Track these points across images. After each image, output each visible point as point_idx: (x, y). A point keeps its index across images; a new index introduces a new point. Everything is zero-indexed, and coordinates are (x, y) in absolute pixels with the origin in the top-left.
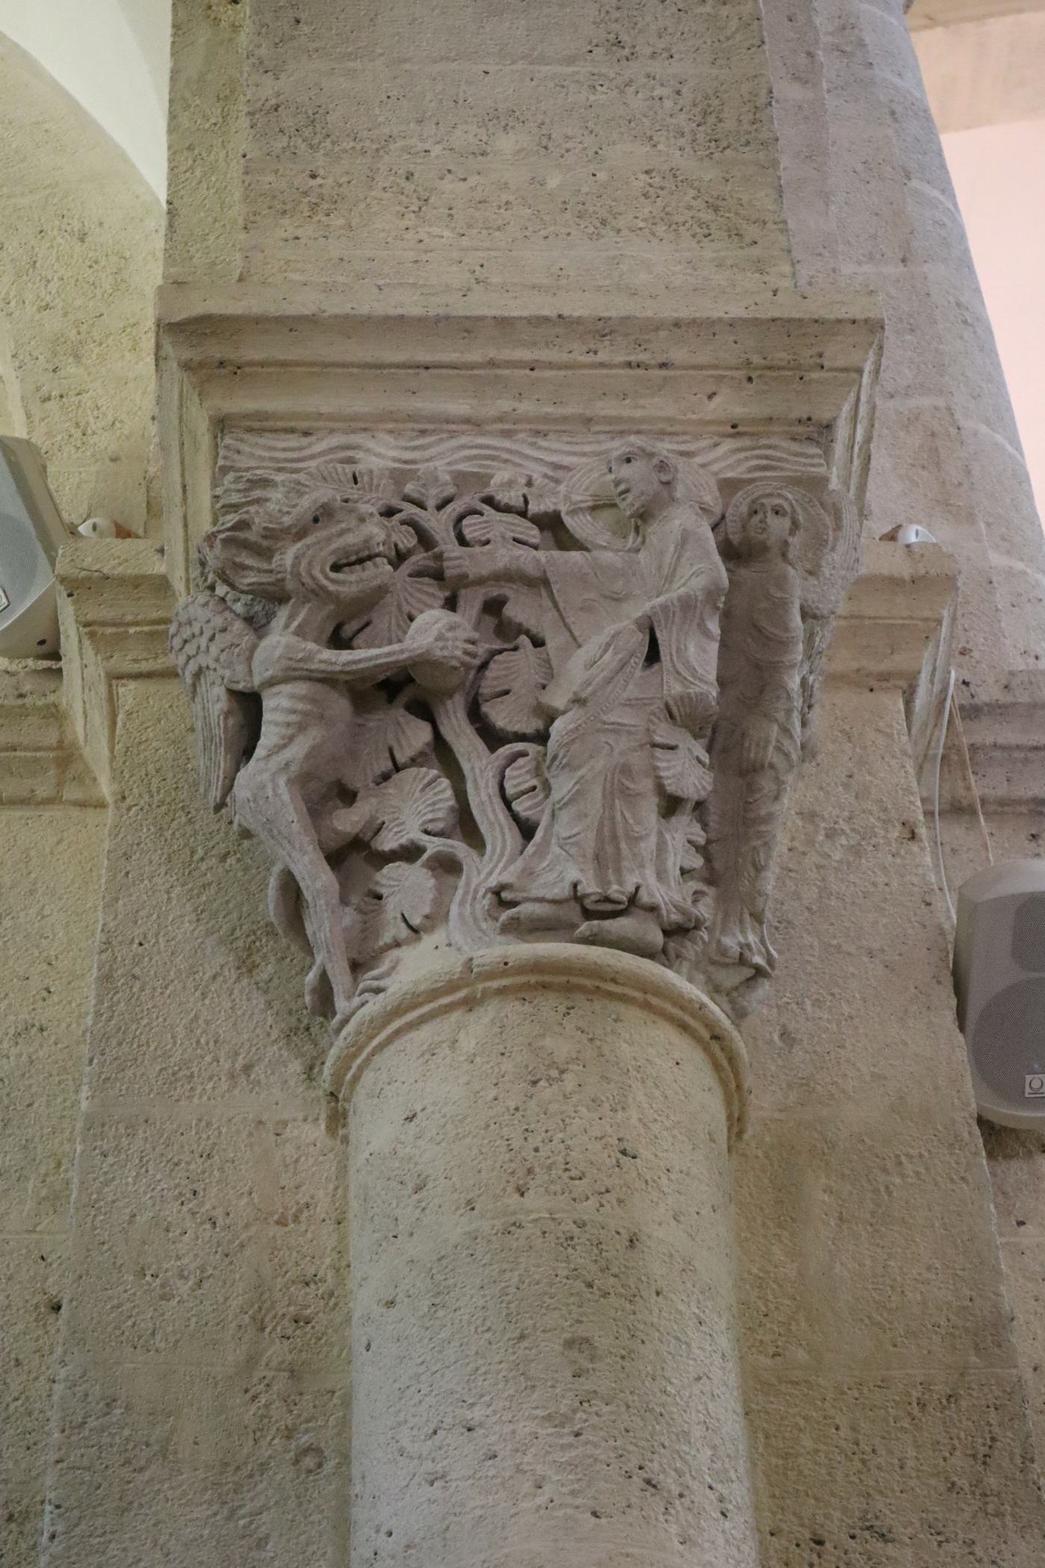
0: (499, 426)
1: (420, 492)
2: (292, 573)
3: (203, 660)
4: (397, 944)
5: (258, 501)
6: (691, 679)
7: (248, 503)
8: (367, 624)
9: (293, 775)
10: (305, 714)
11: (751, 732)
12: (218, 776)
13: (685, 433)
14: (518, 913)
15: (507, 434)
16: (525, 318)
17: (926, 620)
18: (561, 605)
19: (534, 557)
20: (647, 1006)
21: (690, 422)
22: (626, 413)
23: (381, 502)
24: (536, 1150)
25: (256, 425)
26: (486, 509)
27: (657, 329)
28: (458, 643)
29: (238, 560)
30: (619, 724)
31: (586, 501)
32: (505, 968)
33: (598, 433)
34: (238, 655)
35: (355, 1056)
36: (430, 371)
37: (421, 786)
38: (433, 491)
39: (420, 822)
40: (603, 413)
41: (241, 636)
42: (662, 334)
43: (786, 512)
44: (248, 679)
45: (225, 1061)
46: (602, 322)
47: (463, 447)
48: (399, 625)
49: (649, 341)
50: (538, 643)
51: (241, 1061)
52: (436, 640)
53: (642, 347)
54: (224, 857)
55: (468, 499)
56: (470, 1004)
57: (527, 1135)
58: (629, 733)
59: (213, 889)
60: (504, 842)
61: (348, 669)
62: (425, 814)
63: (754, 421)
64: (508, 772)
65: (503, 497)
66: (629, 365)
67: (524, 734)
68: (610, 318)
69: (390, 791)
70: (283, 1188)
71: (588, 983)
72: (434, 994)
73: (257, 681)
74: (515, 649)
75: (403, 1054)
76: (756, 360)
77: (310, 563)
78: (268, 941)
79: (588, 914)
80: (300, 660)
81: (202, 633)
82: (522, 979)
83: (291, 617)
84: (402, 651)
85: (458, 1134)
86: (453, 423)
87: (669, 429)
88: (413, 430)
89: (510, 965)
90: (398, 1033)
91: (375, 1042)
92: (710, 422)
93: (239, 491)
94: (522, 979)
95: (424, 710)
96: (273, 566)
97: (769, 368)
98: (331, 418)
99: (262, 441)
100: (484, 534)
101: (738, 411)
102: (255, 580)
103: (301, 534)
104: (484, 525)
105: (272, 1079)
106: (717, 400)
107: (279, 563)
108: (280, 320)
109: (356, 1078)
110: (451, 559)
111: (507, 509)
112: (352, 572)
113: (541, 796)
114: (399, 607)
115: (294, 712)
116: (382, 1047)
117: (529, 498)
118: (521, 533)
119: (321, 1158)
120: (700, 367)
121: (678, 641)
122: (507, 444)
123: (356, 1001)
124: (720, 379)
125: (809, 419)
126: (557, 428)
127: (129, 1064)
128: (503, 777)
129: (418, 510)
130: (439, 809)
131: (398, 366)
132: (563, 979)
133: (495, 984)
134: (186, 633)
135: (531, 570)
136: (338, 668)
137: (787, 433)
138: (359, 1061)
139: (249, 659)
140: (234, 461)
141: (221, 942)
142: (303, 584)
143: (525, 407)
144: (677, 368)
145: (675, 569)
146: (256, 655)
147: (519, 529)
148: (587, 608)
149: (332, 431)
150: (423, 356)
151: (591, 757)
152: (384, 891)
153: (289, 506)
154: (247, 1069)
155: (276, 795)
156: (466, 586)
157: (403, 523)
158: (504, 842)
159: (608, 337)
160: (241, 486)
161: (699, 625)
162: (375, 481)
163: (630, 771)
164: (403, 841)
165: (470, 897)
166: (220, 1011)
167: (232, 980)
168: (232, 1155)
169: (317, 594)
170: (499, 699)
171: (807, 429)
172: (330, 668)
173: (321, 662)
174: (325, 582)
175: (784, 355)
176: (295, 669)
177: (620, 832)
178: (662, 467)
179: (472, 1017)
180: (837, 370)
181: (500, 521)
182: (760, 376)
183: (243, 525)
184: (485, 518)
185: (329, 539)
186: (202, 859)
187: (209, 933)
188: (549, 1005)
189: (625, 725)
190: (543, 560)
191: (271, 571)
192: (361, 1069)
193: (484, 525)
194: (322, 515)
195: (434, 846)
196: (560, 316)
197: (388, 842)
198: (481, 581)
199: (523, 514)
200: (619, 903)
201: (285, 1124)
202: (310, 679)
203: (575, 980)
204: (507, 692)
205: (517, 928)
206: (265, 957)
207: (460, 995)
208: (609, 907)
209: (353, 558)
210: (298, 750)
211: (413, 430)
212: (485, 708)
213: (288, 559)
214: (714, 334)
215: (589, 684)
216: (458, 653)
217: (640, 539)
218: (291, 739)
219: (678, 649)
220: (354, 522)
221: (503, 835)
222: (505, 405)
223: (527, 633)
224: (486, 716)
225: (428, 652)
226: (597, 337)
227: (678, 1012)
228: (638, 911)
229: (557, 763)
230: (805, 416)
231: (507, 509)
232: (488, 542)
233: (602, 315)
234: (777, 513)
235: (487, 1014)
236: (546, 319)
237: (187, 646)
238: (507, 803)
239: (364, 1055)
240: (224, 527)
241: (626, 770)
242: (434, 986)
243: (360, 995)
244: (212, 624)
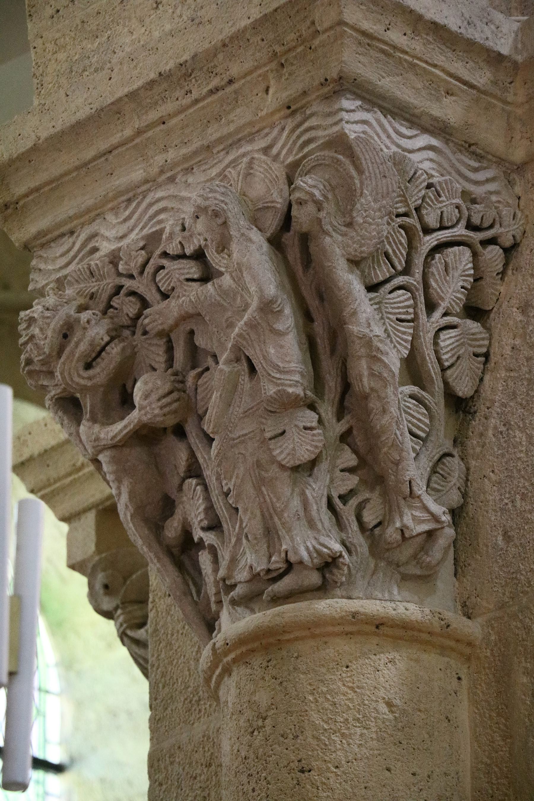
0: (164, 177)
6: (278, 376)
13: (264, 128)
14: (232, 597)
16: (142, 87)
20: (314, 636)
21: (262, 119)
22: (225, 131)
23: (110, 286)
25: (44, 240)
27: (215, 55)
28: (153, 406)
29: (40, 383)
30: (243, 435)
38: (132, 265)
42: (220, 56)
49: (215, 66)
58: (251, 439)
63: (295, 100)
66: (212, 92)
68: (186, 61)
74: (207, 369)
76: (278, 49)
87: (254, 130)
88: (123, 202)
92: (272, 114)
94: (238, 652)
97: (289, 50)
100: (169, 284)
101: (285, 96)
104: (167, 277)
108: (20, 158)
117: (183, 243)
118: (188, 273)
121: (261, 350)
125: (326, 80)
127: (169, 701)
143: (171, 155)
150: (103, 146)
151: (235, 468)
161: (270, 330)
171: (329, 88)
178: (216, 214)
180: (326, 30)
181: (175, 269)
182: (286, 60)
185: (72, 353)
189: (246, 435)
193: (167, 277)
198: (176, 325)
200: (280, 568)
202: (109, 448)
208: (274, 574)
211: (123, 202)
216: (157, 411)
219: (264, 356)
222: (159, 159)
225: (140, 421)
227: (337, 629)
230: (323, 80)
234: (301, 204)
236: (151, 84)
241: (258, 464)
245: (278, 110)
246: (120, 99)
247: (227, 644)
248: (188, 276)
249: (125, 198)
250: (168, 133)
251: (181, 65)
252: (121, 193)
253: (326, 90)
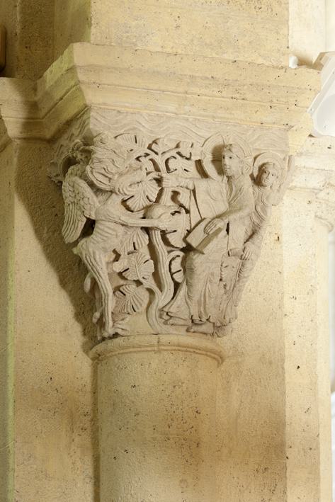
17: (298, 145)
26: (178, 156)
42: (246, 87)
50: (188, 212)
55: (174, 153)
71: (192, 350)
82: (174, 348)
94: (174, 348)
114: (144, 192)
132: (185, 349)
157: (151, 160)
177: (207, 294)
196: (212, 77)
203: (188, 349)
204: (175, 231)
206: (69, 281)
212: (168, 236)
223: (184, 207)
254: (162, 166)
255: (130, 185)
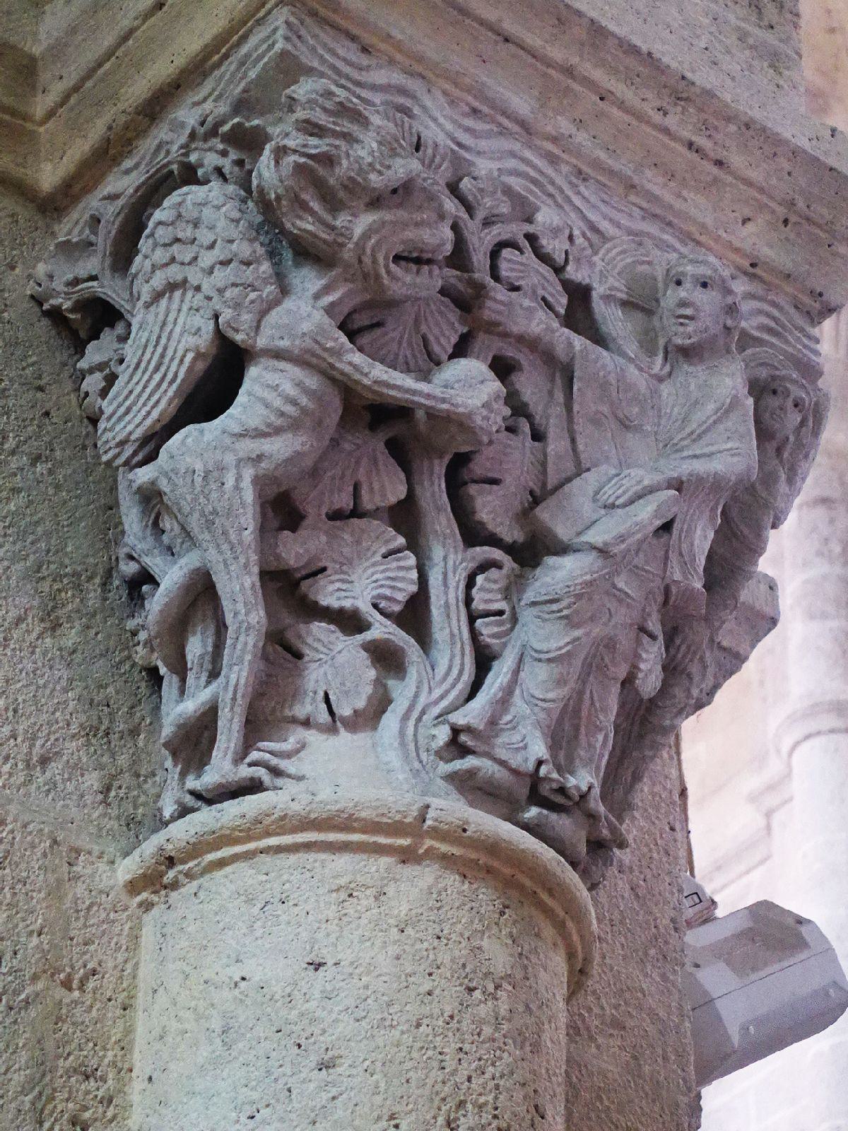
0: (549, 146)
1: (475, 197)
2: (357, 244)
3: (194, 276)
4: (306, 723)
5: (347, 137)
7: (336, 134)
8: (379, 325)
9: (261, 472)
10: (304, 411)
11: (687, 629)
12: (149, 413)
15: (553, 160)
16: (619, 38)
18: (576, 408)
19: (568, 338)
21: (717, 239)
22: (668, 197)
24: (469, 1079)
26: (525, 244)
27: (729, 119)
29: (305, 196)
31: (621, 291)
32: (457, 834)
33: (634, 204)
34: (252, 302)
35: (236, 841)
36: (510, 45)
37: (383, 550)
39: (375, 593)
40: (649, 186)
41: (266, 281)
42: (732, 128)
43: (804, 406)
44: (252, 334)
45: (23, 741)
46: (684, 83)
47: (513, 154)
48: (410, 344)
50: (538, 436)
51: (37, 751)
52: (483, 406)
53: (708, 133)
54: (36, 459)
55: (515, 230)
56: (407, 856)
57: (461, 1055)
59: (21, 499)
60: (462, 664)
61: (376, 388)
62: (382, 586)
63: (772, 270)
64: (480, 579)
65: (549, 244)
66: (690, 145)
67: (502, 540)
68: (693, 84)
69: (346, 536)
70: (72, 939)
72: (374, 827)
73: (261, 342)
75: (308, 875)
76: (801, 204)
77: (378, 243)
78: (73, 596)
79: (536, 797)
80: (326, 350)
81: (212, 246)
83: (327, 290)
84: (444, 400)
85: (383, 1019)
86: (508, 117)
87: (697, 236)
88: (467, 104)
89: (468, 833)
90: (308, 846)
91: (273, 841)
92: (737, 250)
93: (325, 110)
95: (400, 453)
96: (338, 223)
97: (808, 219)
98: (398, 46)
99: (317, 31)
101: (766, 252)
102: (310, 227)
103: (376, 202)
105: (70, 787)
106: (749, 226)
107: (346, 224)
109: (222, 863)
110: (495, 300)
111: (544, 258)
112: (407, 270)
113: (509, 626)
114: (417, 322)
115: (294, 403)
116: (279, 849)
118: (553, 295)
119: (112, 915)
120: (750, 184)
122: (550, 171)
123: (245, 772)
124: (762, 207)
125: (821, 295)
126: (600, 178)
128: (470, 583)
129: (466, 216)
130: (400, 590)
131: (482, 23)
132: (507, 871)
133: (444, 848)
134: (186, 232)
135: (560, 351)
136: (366, 381)
137: (795, 297)
138: (238, 849)
139: (264, 313)
140: (295, 46)
141: (25, 577)
142: (360, 261)
143: (581, 137)
144: (731, 173)
145: (704, 432)
146: (274, 313)
147: (550, 289)
148: (596, 421)
149: (392, 62)
150: (509, 26)
151: (592, 619)
152: (306, 651)
153: (382, 165)
154: (44, 761)
155: (237, 488)
156: (488, 332)
158: (462, 664)
159: (682, 103)
160: (329, 104)
162: (437, 160)
163: (614, 648)
164: (347, 604)
165: (415, 715)
166: (21, 671)
167: (34, 635)
168: (24, 874)
169: (369, 277)
170: (487, 486)
172: (357, 376)
173: (350, 363)
174: (383, 271)
175: (825, 211)
176: (318, 357)
179: (409, 870)
183: (327, 160)
184: (520, 258)
185: (405, 225)
186: (13, 453)
187: (15, 559)
188: (486, 897)
190: (578, 348)
191: (333, 228)
192: (235, 858)
194: (402, 192)
195: (381, 629)
196: (650, 54)
197: (329, 594)
198: (505, 335)
199: (558, 270)
201: (78, 852)
205: (467, 784)
207: (404, 842)
208: (559, 799)
209: (415, 255)
210: (279, 448)
211: (467, 104)
212: (473, 489)
213: (358, 231)
214: (775, 154)
215: (623, 541)
217: (667, 368)
218: (278, 431)
220: (434, 216)
221: (463, 655)
222: (564, 125)
224: (472, 498)
225: (469, 415)
226: (673, 98)
228: (578, 813)
229: (555, 607)
231: (544, 258)
232: (516, 289)
233: (689, 75)
235: (425, 876)
236: (634, 50)
237: (176, 247)
238: (472, 619)
239: (251, 846)
240: (305, 150)
241: (610, 644)
242: (377, 820)
243: (250, 765)
244: (234, 246)
245: (747, 256)
246: (579, 14)
247: (465, 830)
248: (550, 299)
249: (476, 104)
250: (599, 115)
251: (683, 78)
252: (480, 94)
253: (807, 300)
254: (480, 259)
255: (398, 258)
